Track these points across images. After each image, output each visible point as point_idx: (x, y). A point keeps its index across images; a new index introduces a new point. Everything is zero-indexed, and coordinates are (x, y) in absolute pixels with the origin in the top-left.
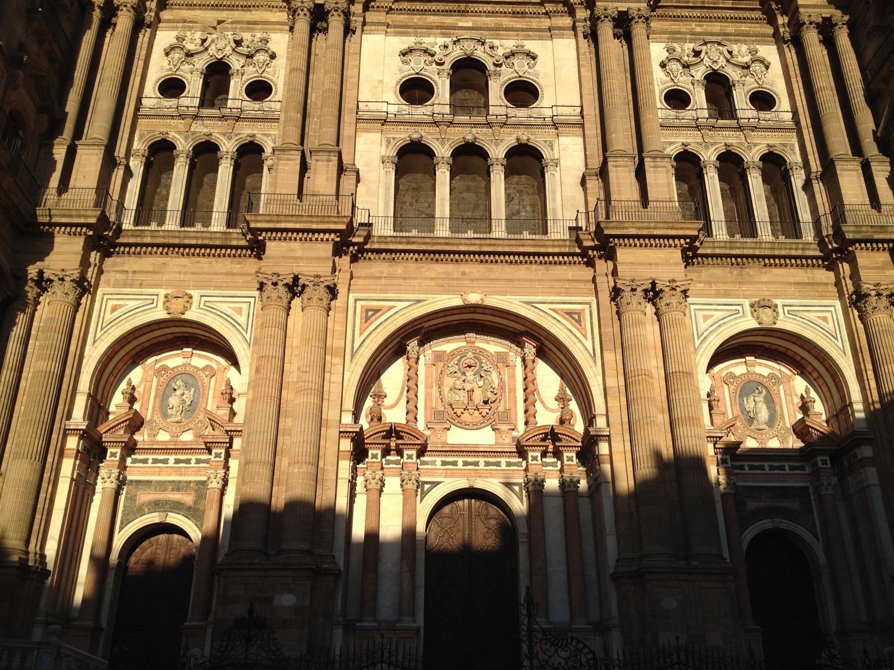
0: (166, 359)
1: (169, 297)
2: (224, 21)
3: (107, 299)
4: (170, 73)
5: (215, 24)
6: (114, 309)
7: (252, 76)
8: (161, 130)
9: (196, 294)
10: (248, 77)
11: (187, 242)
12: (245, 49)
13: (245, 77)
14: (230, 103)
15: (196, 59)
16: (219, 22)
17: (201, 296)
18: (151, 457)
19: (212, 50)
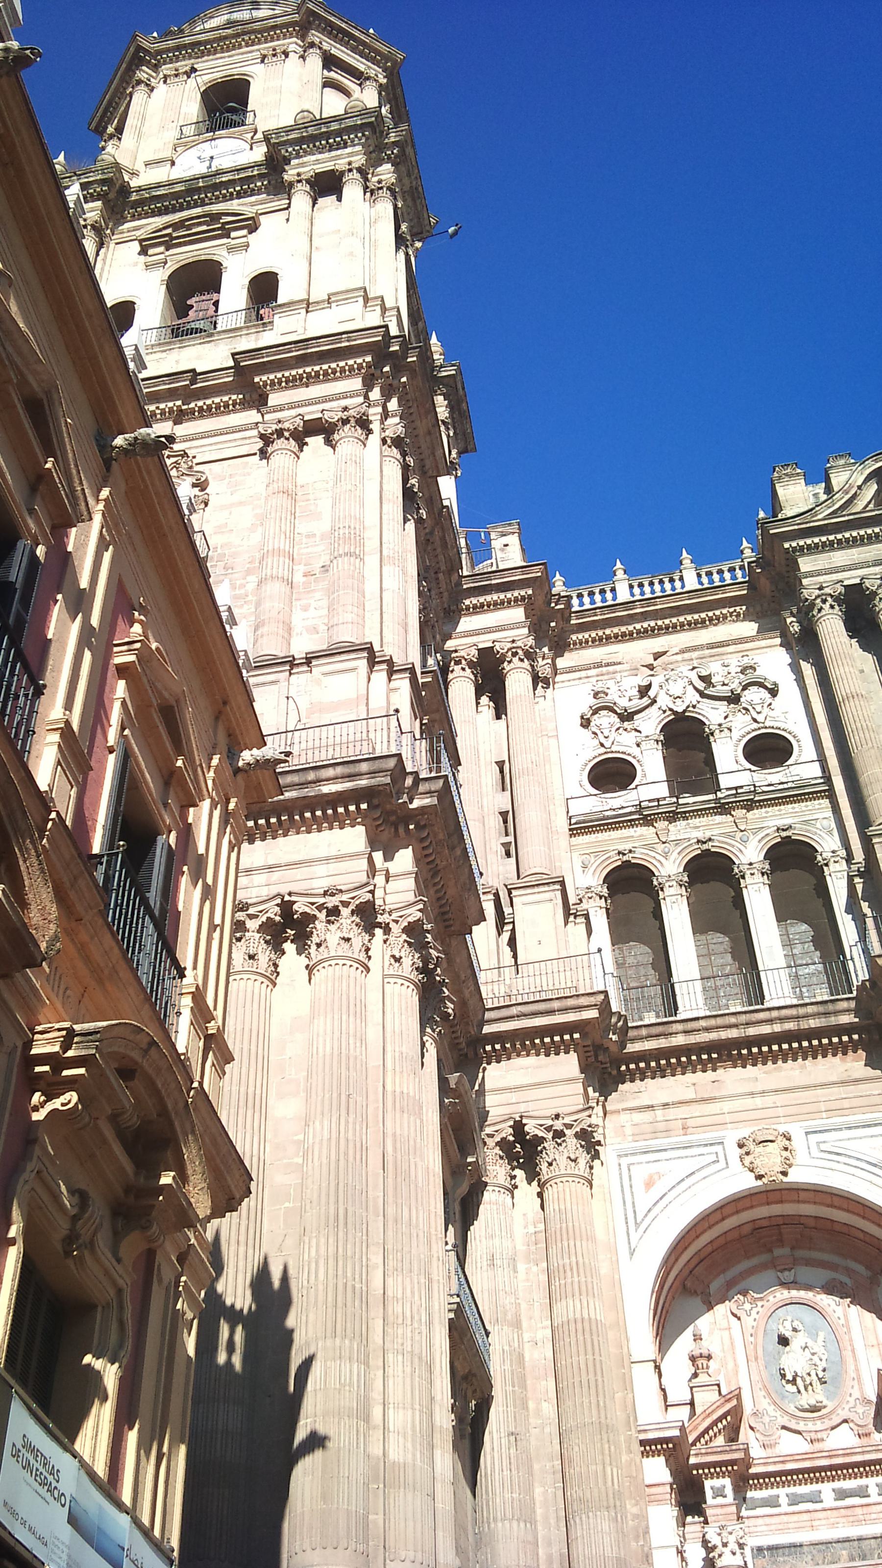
0: (744, 1279)
1: (751, 1146)
2: (665, 653)
3: (629, 1166)
4: (603, 750)
5: (650, 660)
6: (649, 1184)
7: (748, 729)
8: (621, 848)
9: (796, 1130)
10: (742, 732)
11: (752, 1031)
12: (719, 688)
13: (736, 734)
14: (725, 781)
15: (639, 721)
16: (657, 656)
17: (807, 1133)
18: (782, 1492)
19: (664, 701)
